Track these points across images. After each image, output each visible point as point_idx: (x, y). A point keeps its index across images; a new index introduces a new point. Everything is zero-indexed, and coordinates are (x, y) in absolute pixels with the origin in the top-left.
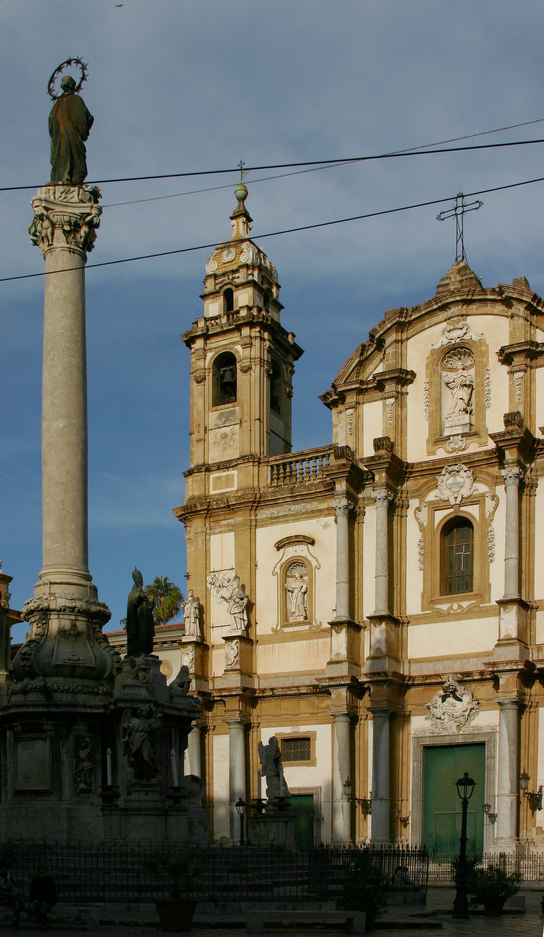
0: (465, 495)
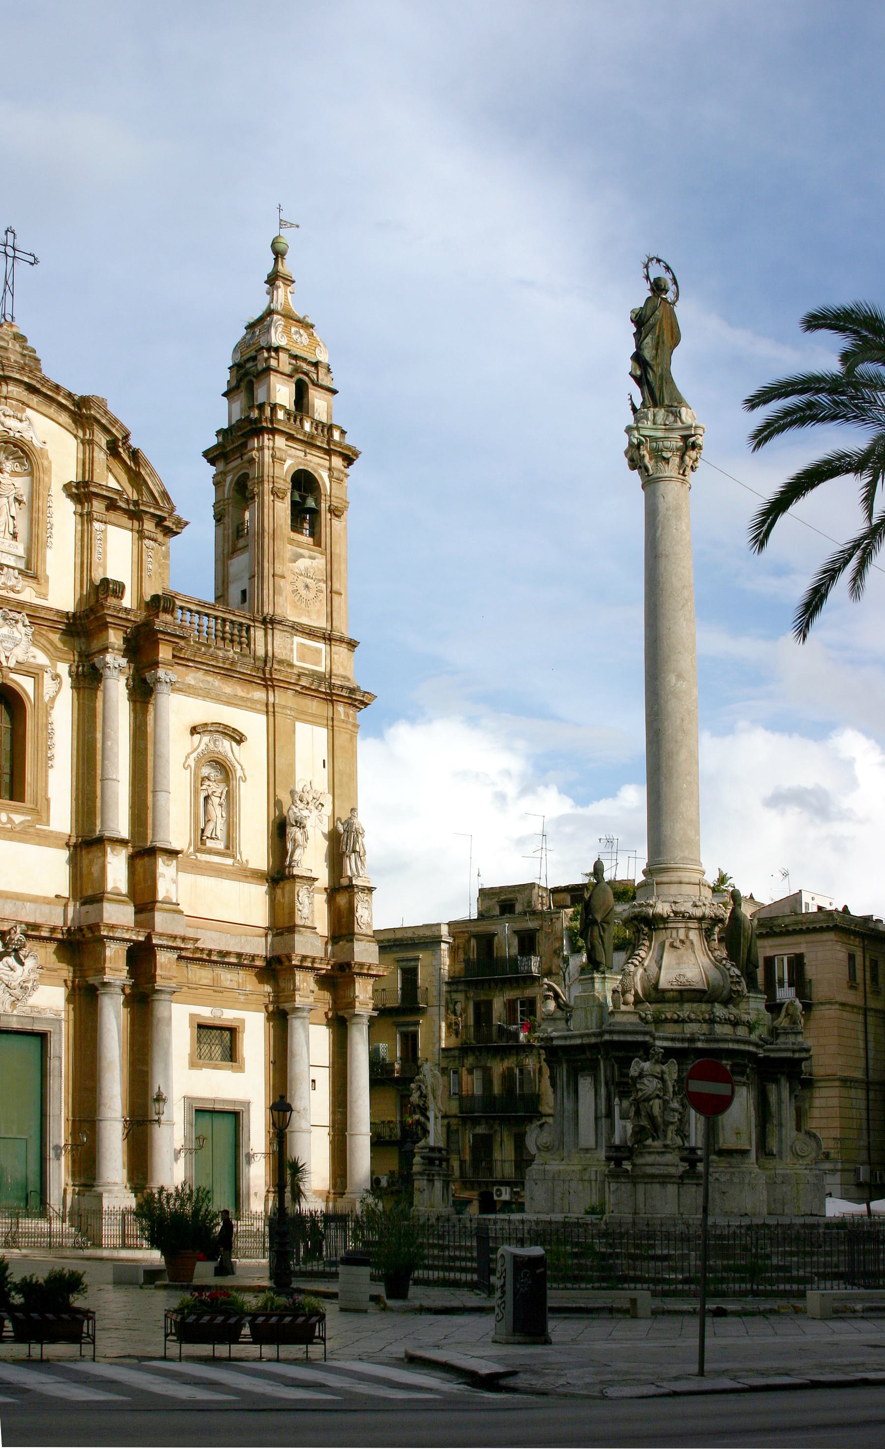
0: (20, 660)
